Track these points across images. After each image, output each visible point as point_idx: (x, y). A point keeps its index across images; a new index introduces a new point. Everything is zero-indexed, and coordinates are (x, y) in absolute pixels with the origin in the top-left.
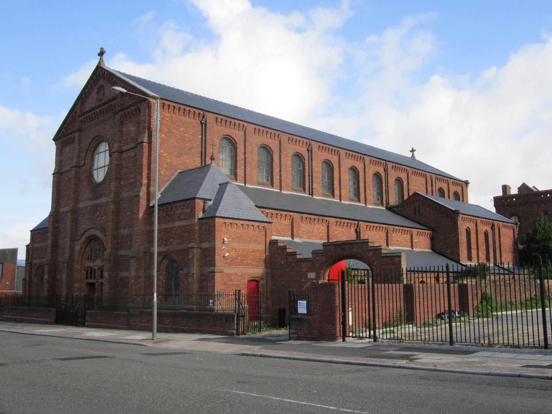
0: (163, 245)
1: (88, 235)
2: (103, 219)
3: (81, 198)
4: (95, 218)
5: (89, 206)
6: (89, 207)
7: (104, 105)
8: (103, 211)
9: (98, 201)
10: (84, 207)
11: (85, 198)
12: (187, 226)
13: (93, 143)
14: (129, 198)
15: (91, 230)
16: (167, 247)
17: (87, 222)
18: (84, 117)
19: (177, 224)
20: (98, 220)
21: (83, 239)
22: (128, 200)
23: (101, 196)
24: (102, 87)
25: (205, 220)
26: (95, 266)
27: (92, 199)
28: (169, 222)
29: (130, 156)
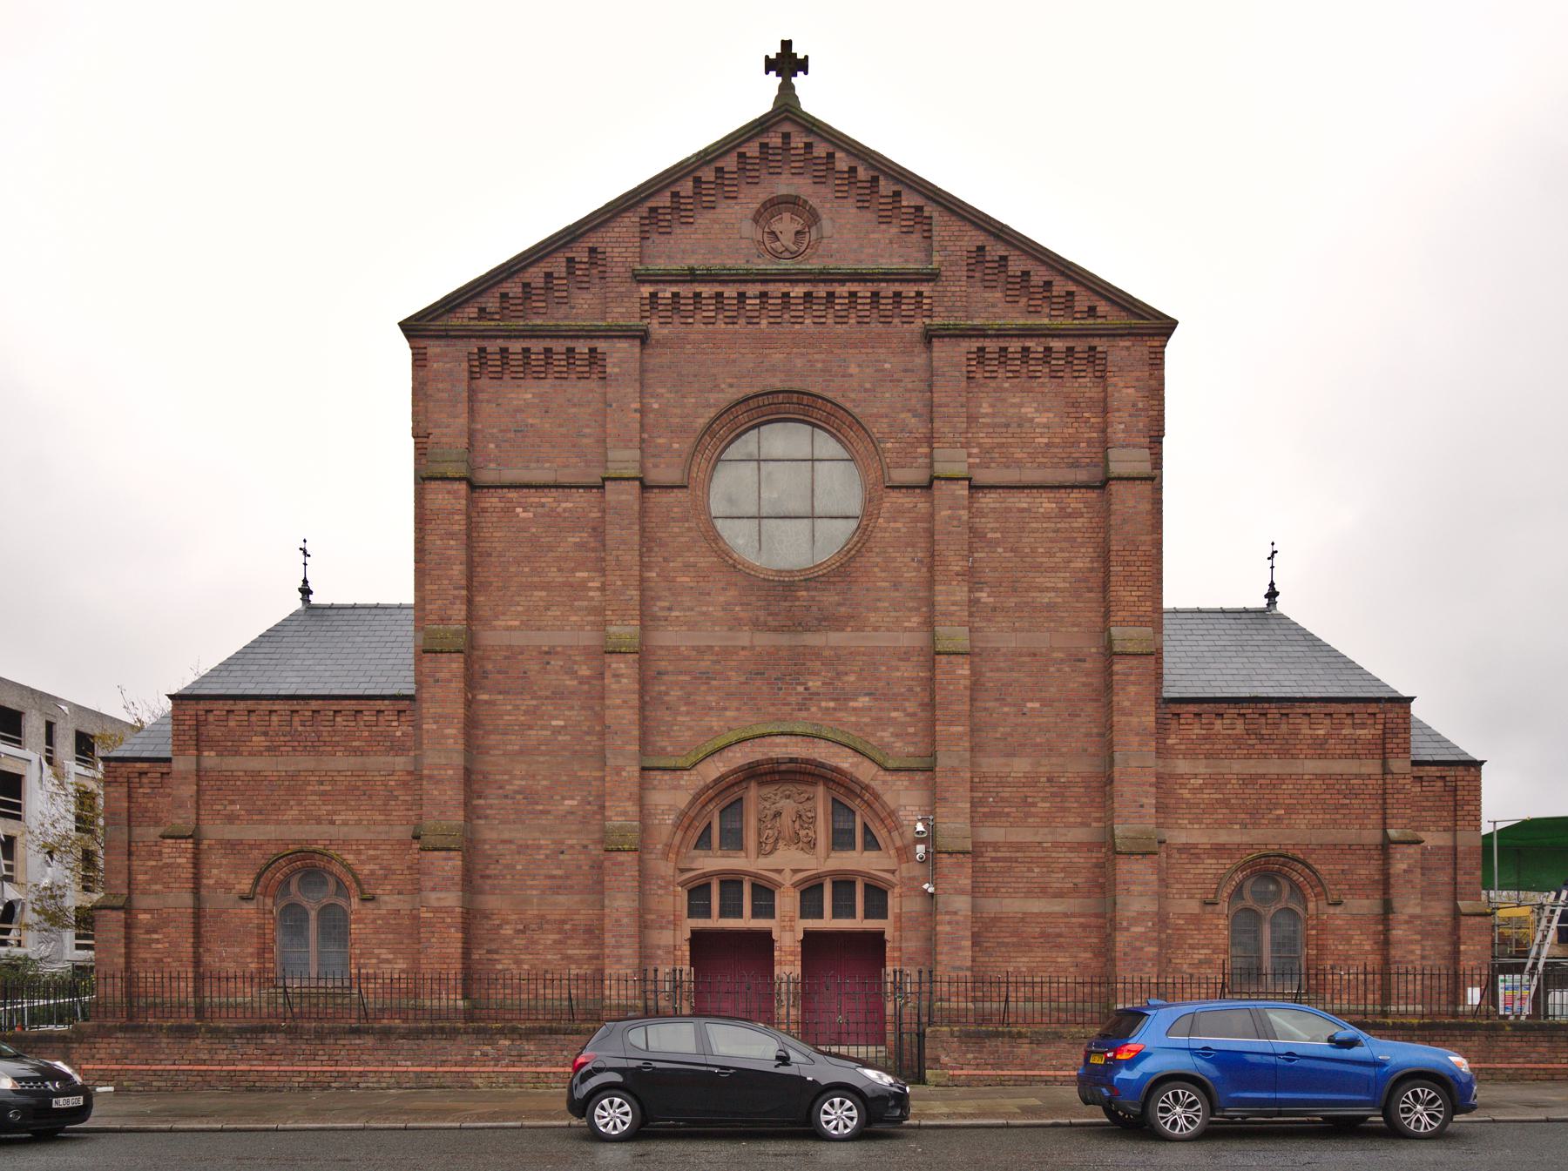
0: (1238, 826)
1: (759, 757)
2: (855, 709)
3: (670, 609)
4: (793, 699)
5: (743, 648)
6: (742, 653)
7: (842, 282)
8: (852, 678)
9: (813, 640)
10: (697, 649)
11: (704, 614)
12: (1357, 776)
13: (743, 407)
14: (1035, 655)
15: (778, 740)
16: (1254, 832)
17: (726, 709)
18: (675, 289)
19: (1312, 766)
20: (813, 709)
21: (715, 769)
22: (1027, 659)
23: (831, 622)
24: (793, 203)
25: (1434, 768)
26: (779, 871)
27: (757, 625)
28: (1265, 756)
29: (1028, 510)
